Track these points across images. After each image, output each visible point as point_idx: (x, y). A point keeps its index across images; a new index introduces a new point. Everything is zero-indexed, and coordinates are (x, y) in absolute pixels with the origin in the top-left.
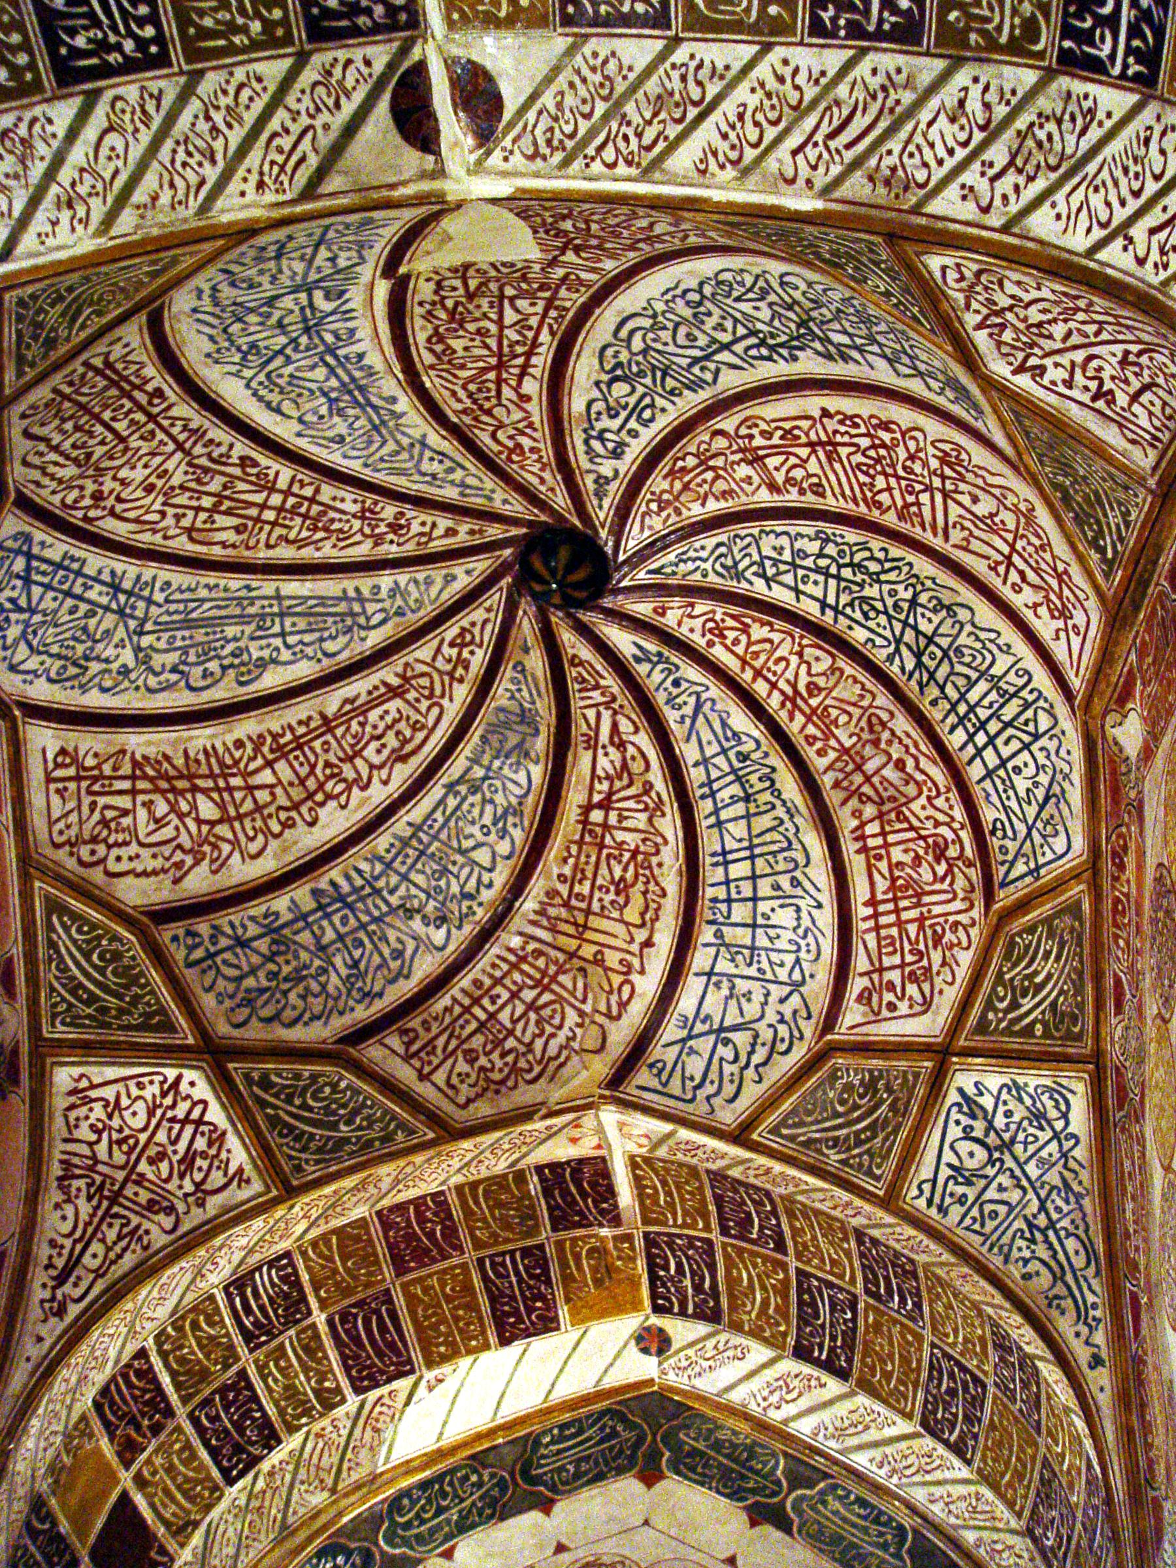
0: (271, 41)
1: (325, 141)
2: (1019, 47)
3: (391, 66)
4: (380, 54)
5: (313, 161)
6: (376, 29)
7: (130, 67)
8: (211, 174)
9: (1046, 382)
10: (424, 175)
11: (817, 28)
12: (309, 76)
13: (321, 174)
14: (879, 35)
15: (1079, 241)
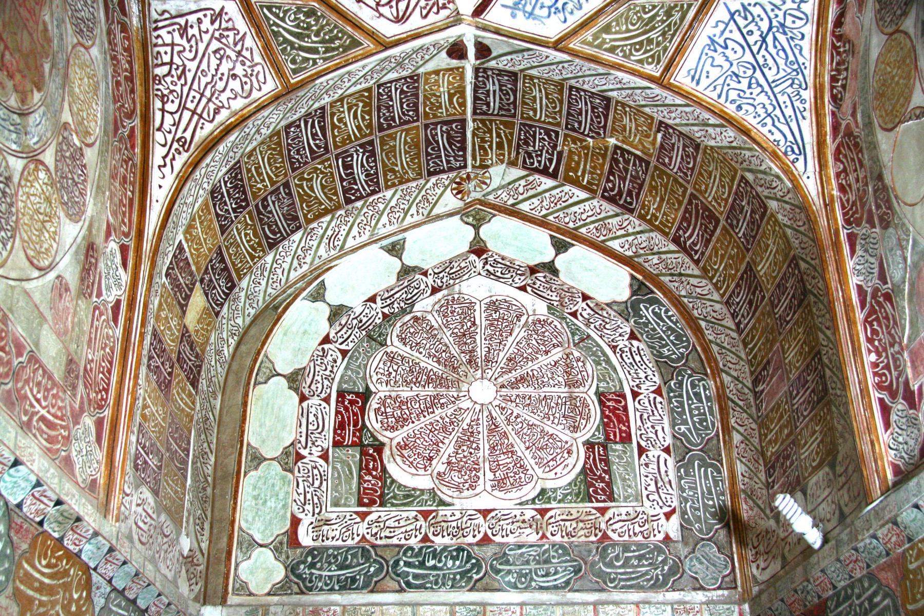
0: (532, 78)
1: (520, 55)
2: (250, 154)
3: (489, 61)
4: (493, 64)
5: (525, 53)
6: (492, 70)
7: (585, 91)
8: (566, 65)
9: (209, 13)
10: (483, 38)
11: (323, 108)
12: (522, 67)
13: (523, 51)
14: (299, 120)
15: (221, 148)
